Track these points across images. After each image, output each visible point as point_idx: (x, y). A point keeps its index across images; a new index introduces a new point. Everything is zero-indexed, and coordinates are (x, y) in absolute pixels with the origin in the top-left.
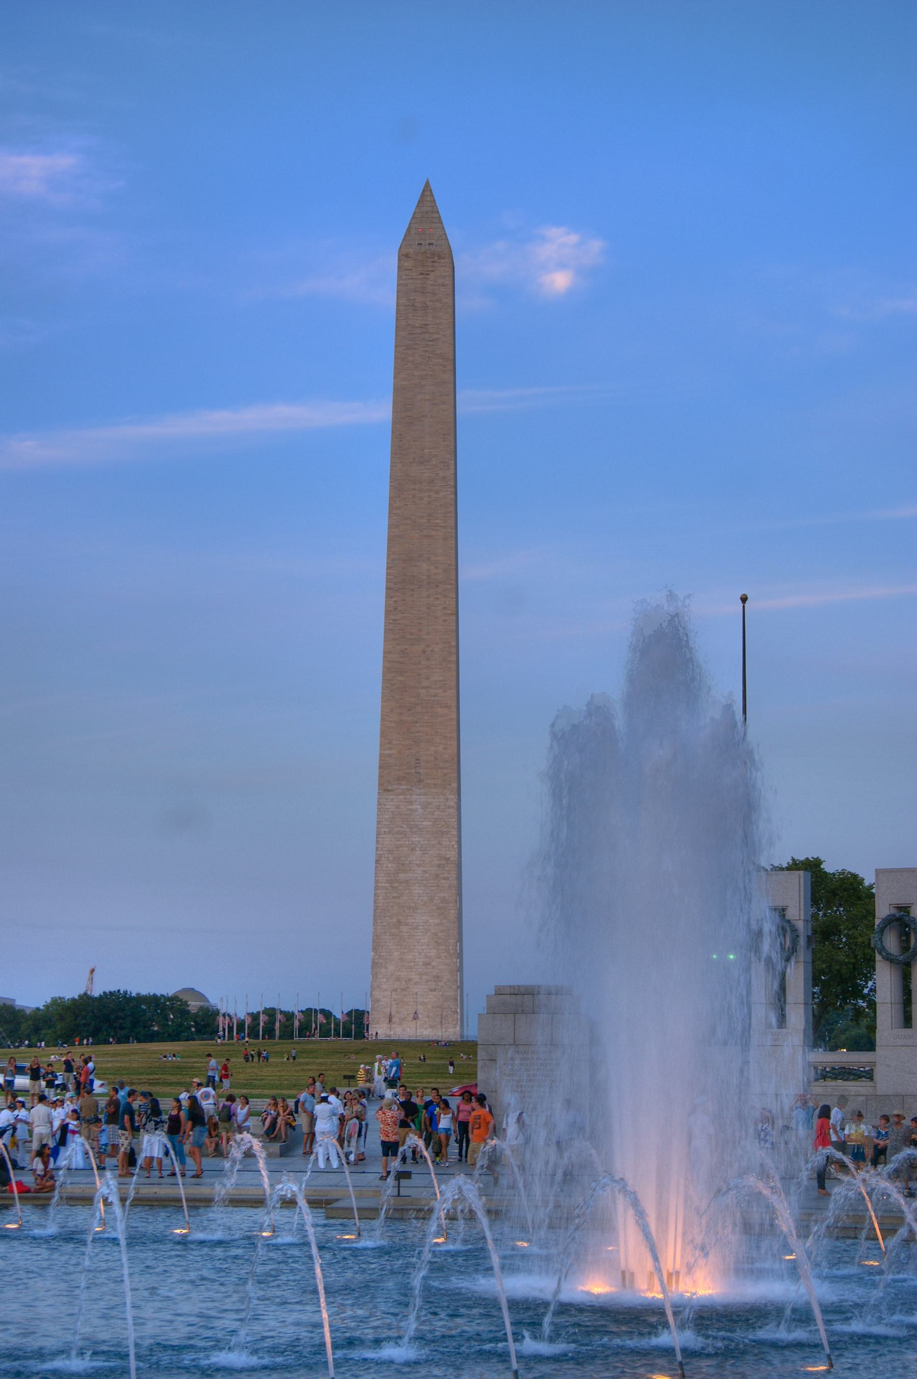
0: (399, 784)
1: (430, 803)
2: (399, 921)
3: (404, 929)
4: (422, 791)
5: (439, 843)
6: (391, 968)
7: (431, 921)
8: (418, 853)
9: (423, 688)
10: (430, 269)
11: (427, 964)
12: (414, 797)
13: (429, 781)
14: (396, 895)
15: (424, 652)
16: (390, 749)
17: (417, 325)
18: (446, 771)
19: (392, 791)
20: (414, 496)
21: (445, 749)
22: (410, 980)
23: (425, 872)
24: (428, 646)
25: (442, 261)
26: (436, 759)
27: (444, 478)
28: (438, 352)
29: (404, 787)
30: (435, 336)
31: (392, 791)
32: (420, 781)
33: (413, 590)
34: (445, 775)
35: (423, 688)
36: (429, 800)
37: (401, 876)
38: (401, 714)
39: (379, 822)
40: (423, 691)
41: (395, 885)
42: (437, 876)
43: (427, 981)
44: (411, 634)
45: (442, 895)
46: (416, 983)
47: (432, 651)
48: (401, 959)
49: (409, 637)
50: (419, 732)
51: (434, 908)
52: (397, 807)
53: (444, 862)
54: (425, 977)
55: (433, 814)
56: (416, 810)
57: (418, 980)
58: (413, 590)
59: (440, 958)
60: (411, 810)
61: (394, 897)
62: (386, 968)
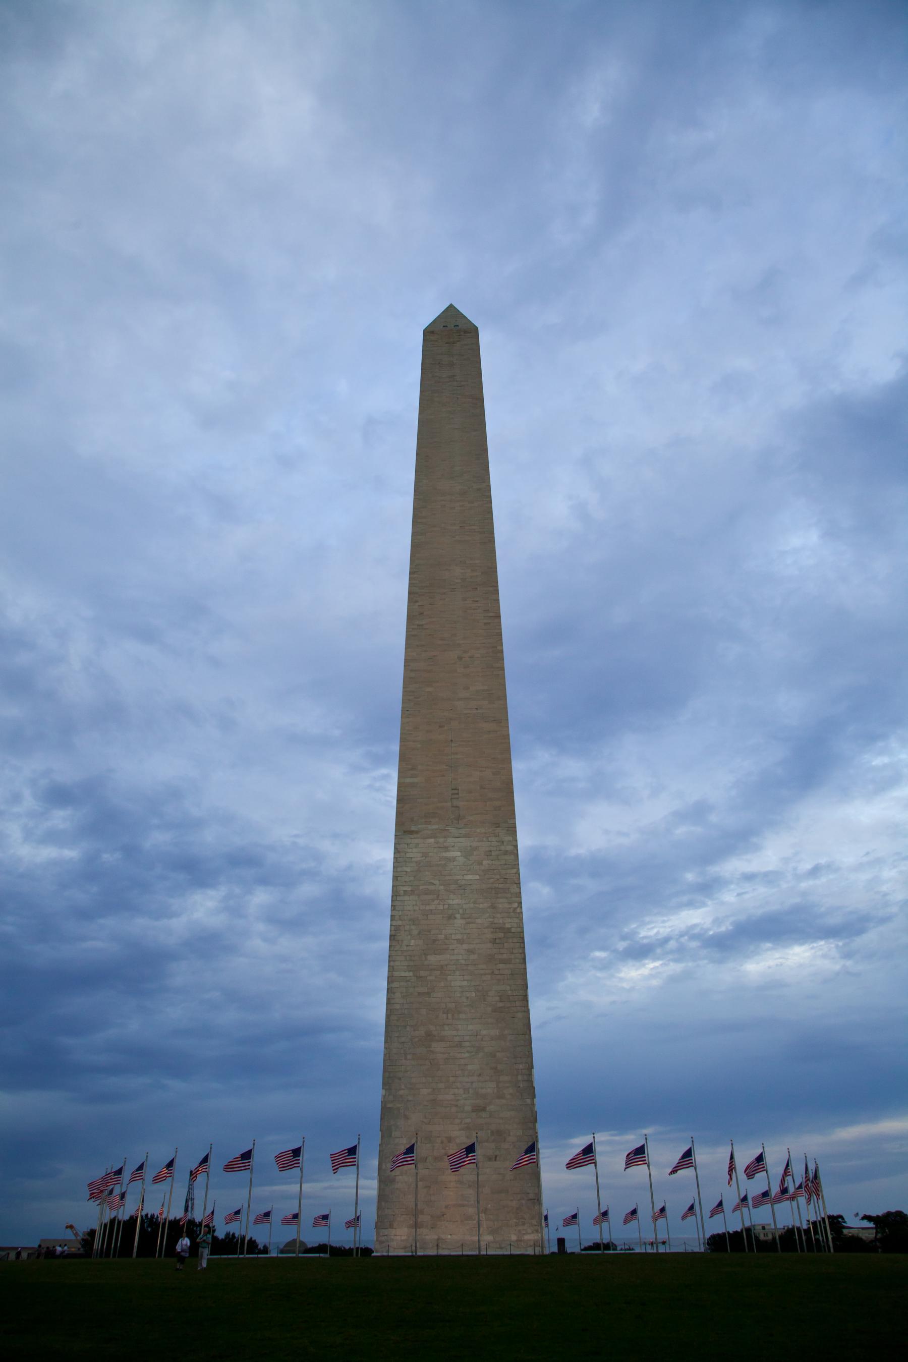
1: (476, 848)
2: (429, 1036)
3: (437, 1047)
4: (463, 831)
5: (493, 907)
7: (484, 1032)
8: (459, 922)
11: (479, 1109)
12: (450, 841)
15: (460, 658)
16: (412, 776)
19: (417, 832)
23: (471, 952)
31: (417, 832)
32: (459, 818)
33: (444, 593)
36: (475, 844)
37: (433, 959)
39: (395, 878)
41: (422, 973)
50: (456, 753)
51: (489, 1009)
52: (425, 855)
53: (501, 935)
55: (480, 863)
56: (454, 859)
58: (444, 593)
59: (500, 1097)
61: (419, 994)
62: (407, 1118)
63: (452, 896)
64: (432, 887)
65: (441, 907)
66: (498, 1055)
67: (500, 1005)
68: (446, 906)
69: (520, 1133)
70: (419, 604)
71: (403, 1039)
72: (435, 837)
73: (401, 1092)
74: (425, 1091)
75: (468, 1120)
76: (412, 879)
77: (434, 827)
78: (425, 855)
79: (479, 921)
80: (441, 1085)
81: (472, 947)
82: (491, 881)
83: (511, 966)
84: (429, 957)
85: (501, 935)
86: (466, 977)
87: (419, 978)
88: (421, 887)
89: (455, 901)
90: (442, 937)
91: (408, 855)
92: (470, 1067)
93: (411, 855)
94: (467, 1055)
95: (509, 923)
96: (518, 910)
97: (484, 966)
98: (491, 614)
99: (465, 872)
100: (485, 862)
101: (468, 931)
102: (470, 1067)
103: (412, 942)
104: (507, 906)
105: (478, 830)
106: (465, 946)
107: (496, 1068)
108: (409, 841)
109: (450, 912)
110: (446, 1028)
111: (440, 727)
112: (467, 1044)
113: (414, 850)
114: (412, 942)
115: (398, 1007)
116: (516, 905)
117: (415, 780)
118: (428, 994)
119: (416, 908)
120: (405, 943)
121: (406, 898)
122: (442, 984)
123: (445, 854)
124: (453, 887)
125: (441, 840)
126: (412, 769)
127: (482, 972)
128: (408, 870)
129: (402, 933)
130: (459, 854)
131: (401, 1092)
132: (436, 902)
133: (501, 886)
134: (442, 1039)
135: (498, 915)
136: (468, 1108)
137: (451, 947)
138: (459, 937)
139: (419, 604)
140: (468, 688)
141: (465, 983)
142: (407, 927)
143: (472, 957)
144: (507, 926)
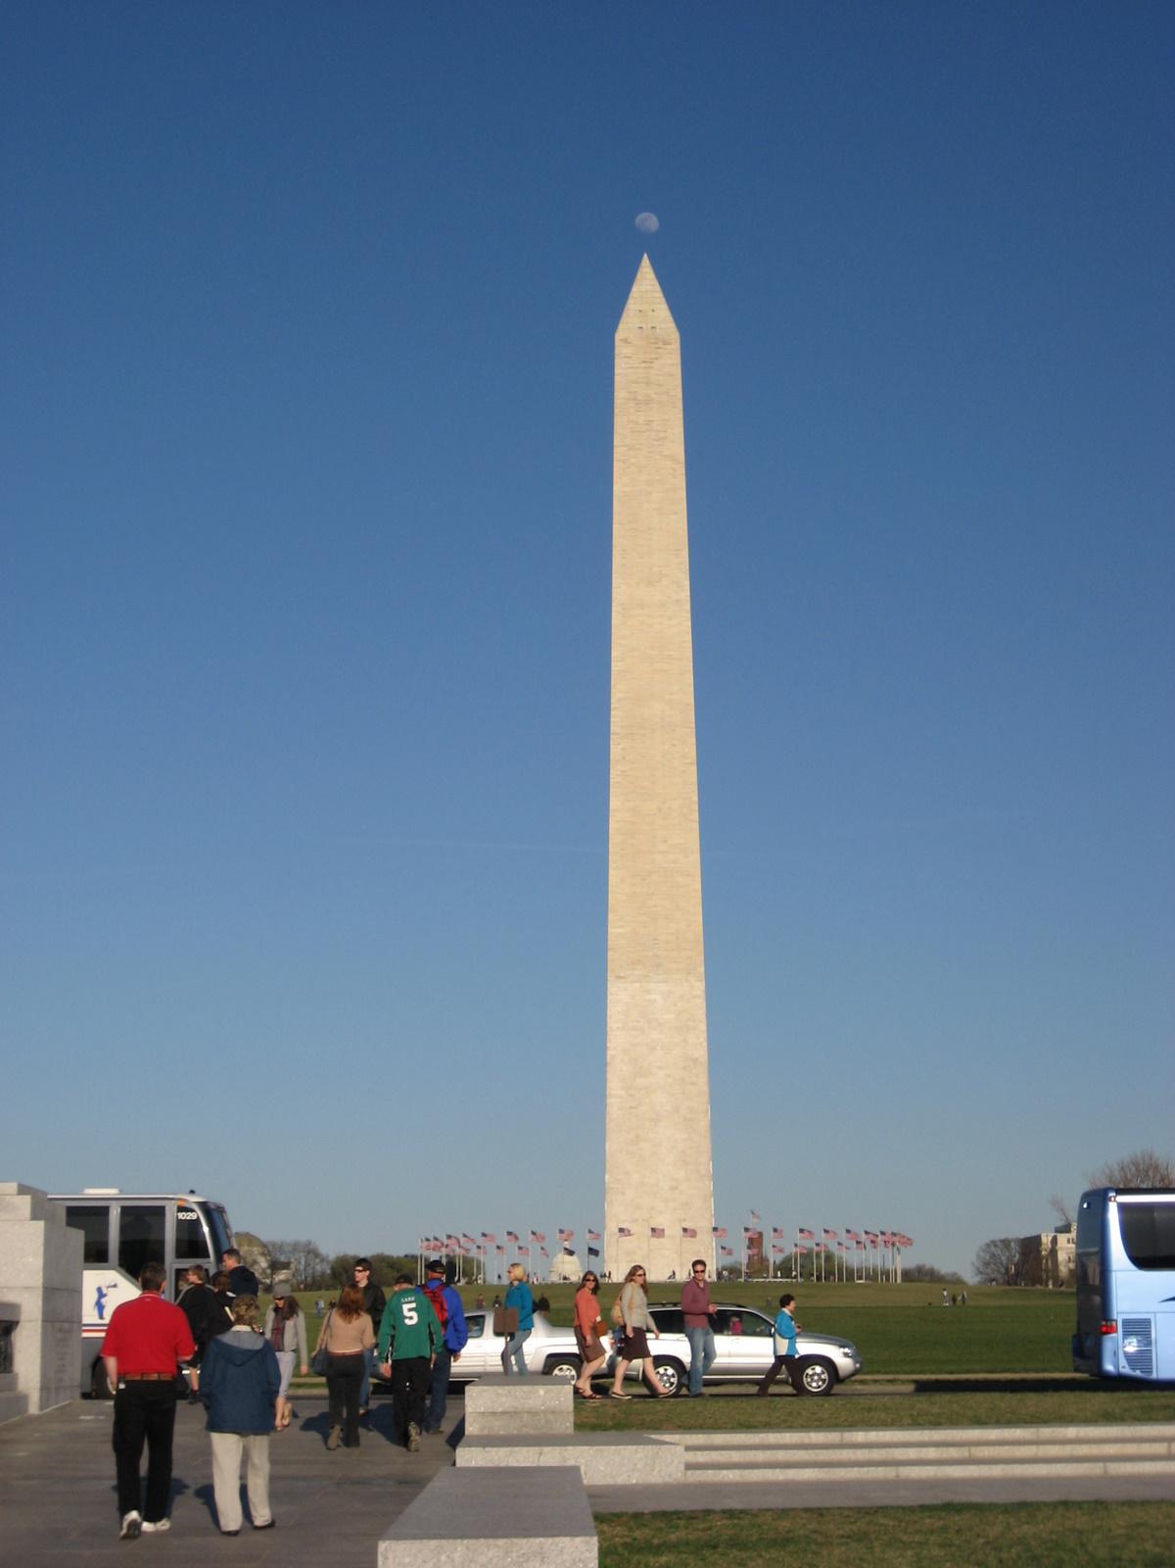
5: (685, 1040)
9: (659, 853)
10: (653, 356)
11: (673, 1189)
15: (660, 810)
17: (641, 421)
22: (653, 1208)
23: (669, 1076)
24: (664, 802)
25: (669, 347)
27: (678, 601)
28: (666, 453)
30: (662, 435)
32: (658, 966)
37: (640, 1081)
41: (631, 1092)
55: (675, 1005)
56: (655, 1000)
61: (631, 1108)
62: (623, 1193)
87: (631, 1095)
98: (689, 761)
114: (624, 1069)
116: (702, 1040)
122: (647, 1100)
123: (648, 997)
139: (620, 747)
140: (665, 841)
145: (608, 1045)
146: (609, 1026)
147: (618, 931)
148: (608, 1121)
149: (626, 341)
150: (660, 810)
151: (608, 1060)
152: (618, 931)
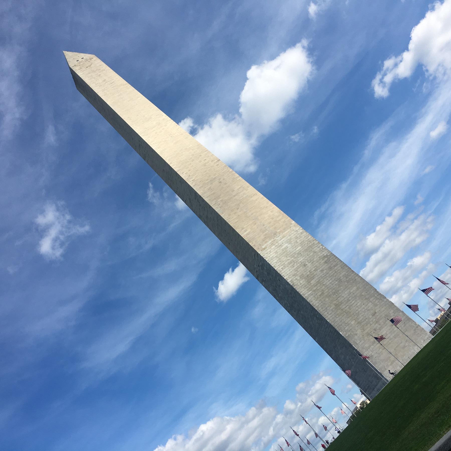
0: (267, 242)
1: (291, 239)
2: (336, 305)
4: (281, 236)
6: (359, 332)
7: (351, 291)
8: (309, 265)
9: (234, 196)
13: (279, 231)
14: (320, 293)
16: (245, 231)
18: (283, 220)
20: (156, 133)
21: (272, 212)
22: (375, 330)
23: (322, 271)
24: (220, 179)
26: (272, 219)
27: (164, 119)
29: (270, 241)
30: (112, 81)
32: (275, 234)
34: (284, 222)
35: (234, 196)
36: (289, 238)
37: (313, 282)
38: (236, 213)
40: (236, 197)
41: (315, 288)
42: (330, 268)
43: (384, 323)
44: (207, 180)
45: (343, 273)
46: (380, 329)
47: (224, 179)
48: (358, 323)
49: (207, 182)
50: (252, 214)
51: (346, 283)
52: (276, 252)
54: (381, 321)
55: (297, 242)
57: (379, 326)
59: (376, 305)
60: (284, 248)
63: (299, 259)
64: (289, 261)
65: (299, 265)
66: (363, 294)
67: (348, 279)
68: (300, 263)
69: (392, 311)
70: (185, 173)
71: (330, 313)
72: (274, 245)
73: (346, 329)
74: (353, 322)
75: (374, 320)
76: (280, 263)
77: (270, 241)
78: (276, 252)
79: (315, 260)
80: (356, 317)
81: (321, 269)
82: (306, 245)
83: (339, 266)
84: (312, 282)
85: (326, 259)
86: (329, 279)
87: (314, 291)
88: (286, 263)
89: (301, 259)
90: (309, 273)
91: (271, 257)
92: (358, 304)
93: (272, 256)
94: (354, 301)
95: (325, 253)
96: (324, 248)
97: (331, 272)
99: (295, 248)
100: (298, 241)
101: (315, 265)
102: (358, 304)
103: (301, 282)
104: (318, 249)
105: (285, 233)
106: (319, 271)
107: (366, 299)
108: (266, 252)
109: (303, 264)
110: (339, 299)
111: (237, 209)
112: (350, 298)
113: (271, 253)
114: (301, 282)
115: (317, 305)
117: (247, 232)
118: (323, 293)
119: (291, 271)
120: (299, 284)
121: (285, 270)
122: (324, 287)
124: (296, 256)
125: (277, 244)
126: (242, 229)
127: (332, 274)
128: (276, 261)
129: (295, 281)
130: (287, 244)
131: (346, 329)
132: (295, 264)
133: (311, 244)
134: (341, 303)
135: (319, 253)
136: (370, 317)
137: (315, 274)
138: (314, 269)
141: (330, 281)
142: (295, 279)
143: (325, 271)
144: (325, 254)
145: (285, 278)
146: (277, 270)
147: (245, 233)
148: (316, 309)
149: (75, 66)
150: (220, 182)
151: (291, 284)
152: (245, 233)
